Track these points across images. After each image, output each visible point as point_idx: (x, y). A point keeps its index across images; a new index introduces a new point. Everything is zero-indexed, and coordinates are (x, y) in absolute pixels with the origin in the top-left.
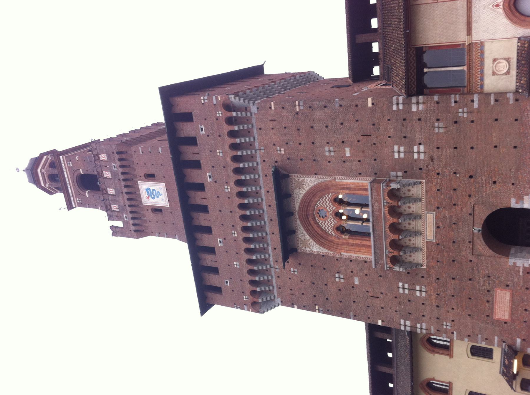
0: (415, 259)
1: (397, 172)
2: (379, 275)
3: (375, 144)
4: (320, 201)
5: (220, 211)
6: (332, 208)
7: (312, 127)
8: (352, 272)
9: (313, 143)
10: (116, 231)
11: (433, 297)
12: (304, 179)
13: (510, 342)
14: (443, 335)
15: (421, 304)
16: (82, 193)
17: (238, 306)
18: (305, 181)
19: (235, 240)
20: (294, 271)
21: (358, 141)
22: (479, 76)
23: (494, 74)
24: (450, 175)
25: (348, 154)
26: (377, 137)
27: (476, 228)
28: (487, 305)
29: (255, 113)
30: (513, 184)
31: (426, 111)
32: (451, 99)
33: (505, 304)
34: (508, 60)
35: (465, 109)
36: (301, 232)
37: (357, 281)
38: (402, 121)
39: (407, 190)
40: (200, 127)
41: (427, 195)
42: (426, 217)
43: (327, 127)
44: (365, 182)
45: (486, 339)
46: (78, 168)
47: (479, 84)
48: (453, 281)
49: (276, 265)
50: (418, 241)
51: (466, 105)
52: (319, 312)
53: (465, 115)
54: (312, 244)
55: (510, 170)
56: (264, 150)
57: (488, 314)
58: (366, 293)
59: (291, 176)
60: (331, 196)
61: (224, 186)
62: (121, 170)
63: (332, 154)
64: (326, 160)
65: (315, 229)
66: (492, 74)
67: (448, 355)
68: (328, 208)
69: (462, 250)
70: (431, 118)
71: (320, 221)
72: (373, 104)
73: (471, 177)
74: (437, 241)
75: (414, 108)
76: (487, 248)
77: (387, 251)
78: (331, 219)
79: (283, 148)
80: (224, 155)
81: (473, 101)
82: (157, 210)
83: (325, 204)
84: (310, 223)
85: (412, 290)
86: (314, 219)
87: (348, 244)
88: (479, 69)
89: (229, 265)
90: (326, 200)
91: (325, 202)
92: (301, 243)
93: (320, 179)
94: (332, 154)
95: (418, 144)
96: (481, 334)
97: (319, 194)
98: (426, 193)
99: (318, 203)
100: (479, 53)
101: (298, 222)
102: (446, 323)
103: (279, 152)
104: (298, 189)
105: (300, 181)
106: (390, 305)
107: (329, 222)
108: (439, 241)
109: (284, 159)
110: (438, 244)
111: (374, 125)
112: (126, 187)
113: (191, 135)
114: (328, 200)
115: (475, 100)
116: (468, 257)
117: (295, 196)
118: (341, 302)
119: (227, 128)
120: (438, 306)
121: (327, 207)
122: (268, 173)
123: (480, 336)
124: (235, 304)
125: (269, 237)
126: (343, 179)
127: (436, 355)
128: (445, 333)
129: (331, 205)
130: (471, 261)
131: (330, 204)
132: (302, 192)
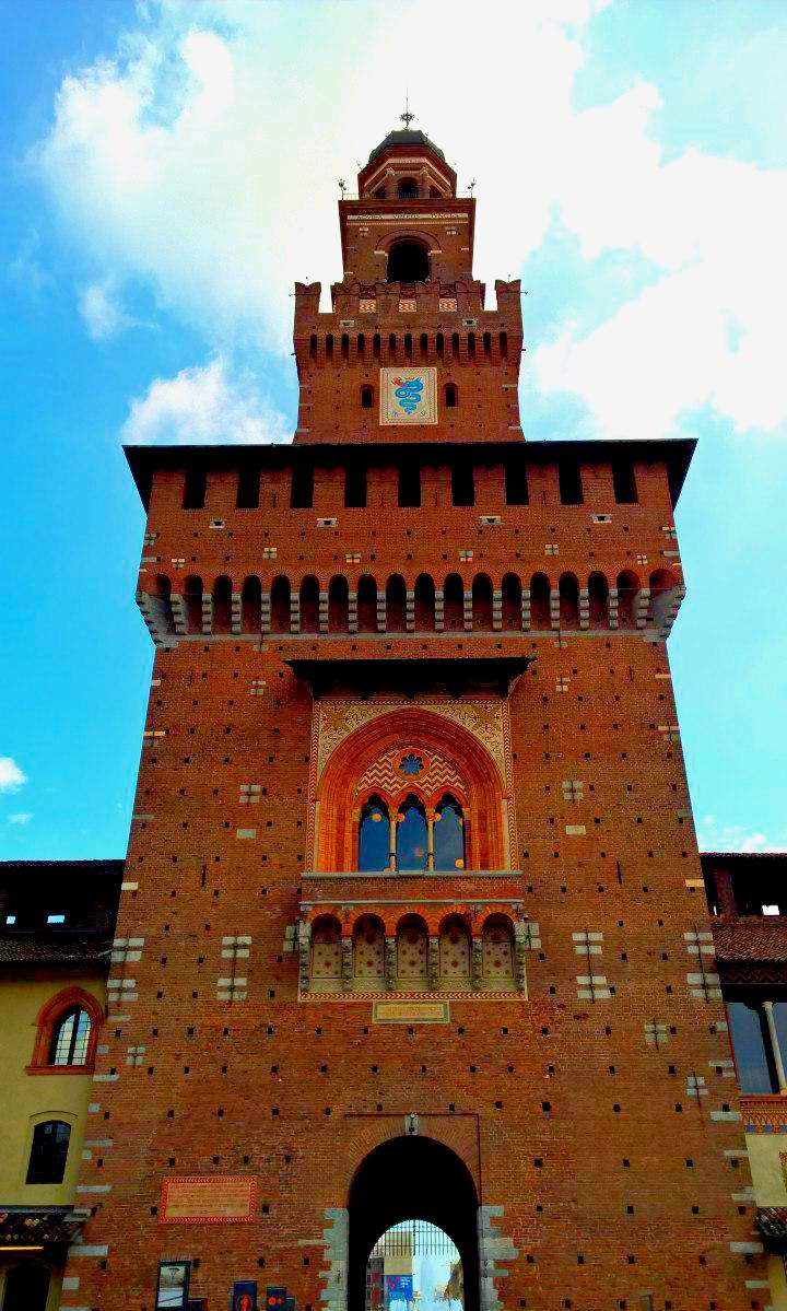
1: (539, 937)
3: (601, 890)
7: (624, 756)
8: (269, 824)
10: (306, 295)
11: (217, 1020)
12: (499, 729)
13: (95, 1226)
15: (195, 989)
16: (386, 241)
17: (152, 543)
18: (497, 732)
20: (257, 687)
21: (603, 855)
22: (775, 1122)
24: (545, 1057)
25: (570, 830)
26: (618, 896)
27: (416, 1121)
28: (207, 1159)
30: (539, 1209)
35: (704, 1092)
37: (244, 834)
40: (608, 516)
41: (492, 1004)
42: (435, 1003)
43: (629, 788)
44: (508, 866)
45: (100, 1163)
50: (366, 984)
51: (714, 1093)
52: (145, 738)
54: (336, 736)
55: (574, 1201)
57: (177, 1161)
62: (463, 334)
63: (567, 796)
67: (35, 1062)
69: (356, 1088)
72: (692, 889)
73: (546, 1107)
75: (694, 978)
76: (366, 1151)
80: (548, 557)
81: (726, 1108)
82: (369, 397)
83: (437, 774)
85: (234, 967)
87: (341, 819)
94: (567, 796)
97: (463, 762)
101: (391, 708)
106: (185, 912)
107: (391, 778)
110: (366, 1031)
112: (424, 337)
113: (585, 493)
114: (447, 780)
117: (456, 706)
119: (611, 572)
120: (191, 1031)
123: (110, 1143)
124: (158, 535)
125: (343, 636)
127: (35, 1030)
130: (328, 1112)
132: (467, 721)
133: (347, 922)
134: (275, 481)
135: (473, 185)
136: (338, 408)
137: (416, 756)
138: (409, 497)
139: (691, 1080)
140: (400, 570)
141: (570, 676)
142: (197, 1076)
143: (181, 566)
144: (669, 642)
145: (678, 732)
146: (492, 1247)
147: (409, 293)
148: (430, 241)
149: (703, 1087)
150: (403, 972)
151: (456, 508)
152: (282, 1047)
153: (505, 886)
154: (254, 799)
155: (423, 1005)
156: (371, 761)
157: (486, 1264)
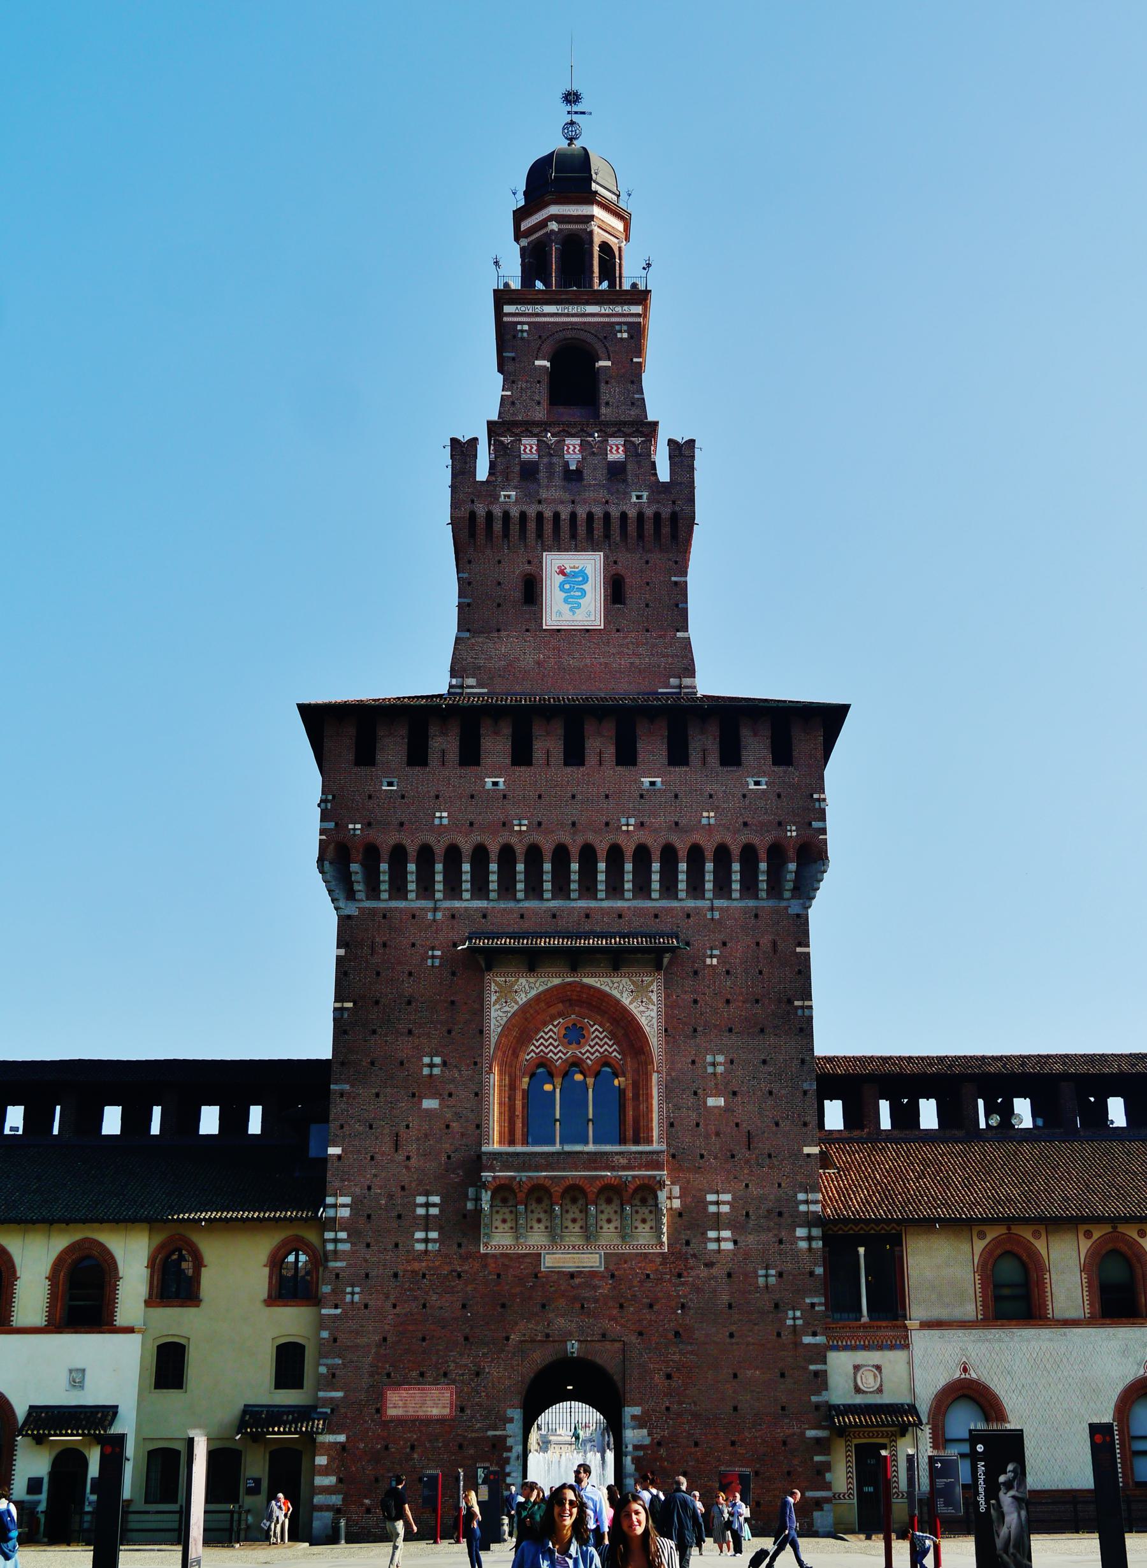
2: (453, 1155)
3: (733, 1156)
4: (603, 1031)
5: (573, 797)
6: (588, 1058)
7: (762, 1030)
8: (450, 1095)
9: (730, 1030)
10: (462, 452)
11: (416, 1266)
14: (329, 1287)
16: (547, 348)
17: (329, 805)
18: (651, 1007)
19: (504, 824)
20: (433, 957)
21: (737, 1125)
22: (853, 1342)
23: (857, 1368)
24: (679, 1296)
25: (711, 1102)
27: (576, 1345)
28: (414, 1374)
31: (796, 1253)
32: (817, 1297)
33: (421, 1407)
34: (880, 1390)
35: (799, 1322)
36: (533, 985)
37: (429, 1104)
38: (777, 1210)
39: (644, 1216)
40: (763, 780)
43: (764, 1062)
47: (840, 1343)
48: (459, 1305)
49: (444, 915)
50: (536, 1239)
51: (807, 1324)
52: (335, 1009)
53: (789, 1322)
56: (712, 919)
58: (405, 1124)
62: (632, 513)
66: (856, 1364)
72: (809, 1155)
74: (543, 1274)
75: (801, 1232)
77: (524, 1179)
78: (565, 1054)
79: (718, 962)
81: (814, 1334)
83: (597, 1043)
85: (427, 1223)
86: (561, 1015)
88: (864, 1342)
89: (437, 797)
90: (606, 1046)
92: (506, 982)
93: (656, 1040)
95: (735, 1238)
96: (343, 1364)
98: (641, 1253)
99: (596, 1026)
100: (891, 1342)
101: (557, 981)
102: (357, 1293)
103: (709, 952)
104: (632, 987)
108: (543, 1277)
109: (694, 962)
110: (536, 1276)
113: (744, 753)
114: (606, 1050)
115: (817, 1338)
116: (515, 1333)
117: (615, 980)
118: (372, 1063)
120: (396, 1275)
121: (590, 1046)
124: (334, 797)
125: (511, 904)
126: (659, 1089)
127: (267, 1270)
128: (333, 1290)
129: (595, 1056)
132: (625, 995)
133: (521, 1191)
134: (444, 734)
135: (649, 265)
136: (499, 605)
137: (579, 1026)
138: (574, 756)
139: (790, 1313)
140: (565, 838)
141: (720, 948)
142: (403, 1311)
143: (358, 832)
145: (811, 1007)
146: (633, 1436)
147: (573, 431)
148: (598, 346)
149: (798, 1318)
150: (567, 1227)
151: (619, 768)
152: (469, 1288)
154: (436, 1071)
156: (538, 1031)
157: (627, 1447)
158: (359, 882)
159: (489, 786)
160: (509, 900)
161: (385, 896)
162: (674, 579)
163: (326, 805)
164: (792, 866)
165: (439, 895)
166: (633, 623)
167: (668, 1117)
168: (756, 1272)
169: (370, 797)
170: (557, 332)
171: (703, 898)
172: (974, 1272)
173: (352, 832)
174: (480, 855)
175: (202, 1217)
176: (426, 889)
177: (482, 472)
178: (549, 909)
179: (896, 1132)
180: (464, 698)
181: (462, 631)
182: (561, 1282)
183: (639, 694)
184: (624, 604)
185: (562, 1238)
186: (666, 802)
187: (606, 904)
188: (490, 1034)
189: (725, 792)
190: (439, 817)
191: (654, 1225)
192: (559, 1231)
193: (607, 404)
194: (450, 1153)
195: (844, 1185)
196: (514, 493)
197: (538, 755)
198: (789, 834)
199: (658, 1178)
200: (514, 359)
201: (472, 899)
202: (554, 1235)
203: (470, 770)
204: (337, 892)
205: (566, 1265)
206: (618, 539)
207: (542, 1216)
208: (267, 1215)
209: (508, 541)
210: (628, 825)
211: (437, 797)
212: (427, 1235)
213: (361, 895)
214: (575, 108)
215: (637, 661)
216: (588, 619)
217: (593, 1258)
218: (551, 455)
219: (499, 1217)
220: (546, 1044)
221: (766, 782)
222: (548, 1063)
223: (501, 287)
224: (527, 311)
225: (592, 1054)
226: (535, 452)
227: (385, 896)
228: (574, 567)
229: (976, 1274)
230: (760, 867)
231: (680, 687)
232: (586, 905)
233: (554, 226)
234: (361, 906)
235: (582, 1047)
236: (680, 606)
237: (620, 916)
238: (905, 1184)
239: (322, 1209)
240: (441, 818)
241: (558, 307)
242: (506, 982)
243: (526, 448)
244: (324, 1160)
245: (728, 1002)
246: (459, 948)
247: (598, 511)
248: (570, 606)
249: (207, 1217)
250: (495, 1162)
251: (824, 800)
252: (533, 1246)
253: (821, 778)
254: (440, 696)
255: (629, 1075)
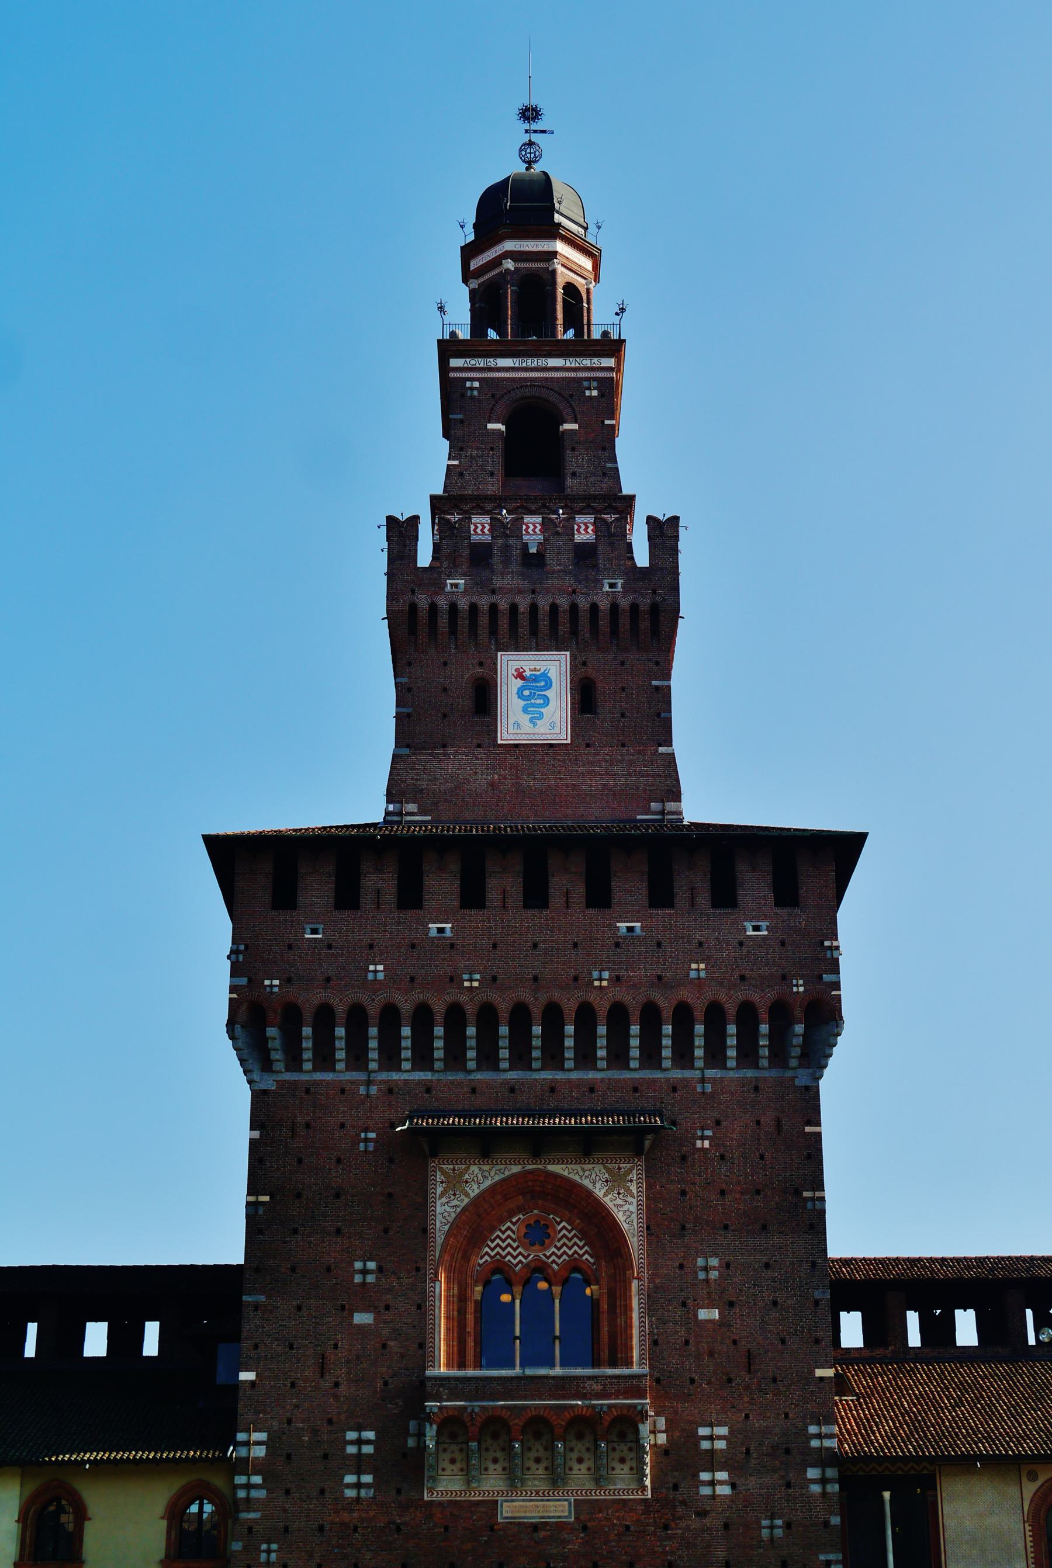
0: (445, 1473)
3: (730, 1381)
5: (535, 946)
7: (764, 1227)
8: (387, 1307)
11: (346, 1517)
17: (241, 958)
18: (630, 1199)
19: (452, 979)
24: (665, 1553)
25: (703, 1314)
29: (796, 1079)
36: (487, 1174)
37: (361, 1318)
40: (764, 924)
43: (767, 1266)
46: (579, 416)
49: (379, 1090)
52: (248, 1204)
54: (455, 1203)
56: (703, 1093)
58: (332, 1343)
59: (639, 1161)
60: (586, 1259)
61: (608, 969)
62: (604, 604)
64: (684, 1258)
65: (494, 1212)
68: (554, 1249)
70: (792, 1509)
71: (516, 1226)
72: (821, 1379)
75: (812, 1473)
77: (477, 1410)
78: (526, 1257)
79: (710, 1145)
83: (564, 1244)
84: (510, 1198)
86: (520, 1210)
89: (371, 946)
90: (576, 1248)
91: (570, 1244)
92: (454, 1170)
93: (636, 1239)
95: (733, 1481)
98: (619, 1499)
99: (564, 1224)
101: (516, 1169)
103: (699, 1133)
104: (607, 1175)
105: (629, 1184)
107: (515, 1249)
108: (500, 1530)
110: (492, 1529)
111: (774, 1380)
113: (740, 892)
114: (576, 1252)
117: (586, 1167)
120: (321, 1528)
121: (556, 1247)
122: (642, 1096)
124: (247, 947)
125: (460, 1076)
126: (639, 1299)
129: (562, 1259)
131: (565, 1257)
132: (598, 1185)
133: (473, 1425)
135: (623, 310)
136: (445, 716)
137: (542, 1223)
140: (525, 995)
141: (712, 1128)
143: (276, 990)
144: (822, 1083)
147: (533, 507)
148: (562, 405)
150: (528, 1469)
151: (590, 911)
153: (632, 1387)
154: (370, 1279)
155: (548, 1503)
158: (278, 1050)
159: (433, 933)
160: (458, 1071)
161: (308, 1066)
162: (654, 683)
163: (237, 958)
164: (799, 1028)
165: (373, 1066)
166: (607, 737)
167: (651, 1333)
168: (759, 1523)
169: (290, 947)
170: (514, 389)
171: (692, 1067)
172: (1024, 1522)
173: (268, 989)
174: (423, 1017)
175: (86, 1458)
176: (358, 1058)
177: (424, 557)
178: (506, 1082)
179: (926, 1350)
180: (403, 827)
181: (400, 747)
182: (522, 1536)
183: (613, 821)
184: (595, 713)
185: (523, 1482)
186: (646, 952)
187: (575, 1075)
188: (435, 1234)
189: (717, 939)
190: (372, 971)
191: (634, 1466)
192: (519, 1474)
193: (574, 474)
194: (387, 1378)
195: (865, 1415)
196: (463, 581)
197: (493, 895)
198: (795, 989)
199: (639, 1408)
200: (462, 421)
201: (413, 1069)
202: (514, 1479)
203: (409, 914)
204: (251, 1061)
205: (528, 1514)
206: (587, 635)
207: (499, 1454)
208: (165, 1455)
209: (456, 638)
210: (601, 979)
211: (371, 946)
212: (359, 1478)
213: (279, 1066)
214: (534, 126)
215: (611, 782)
216: (552, 731)
217: (560, 1506)
218: (507, 536)
219: (447, 1456)
220: (503, 1245)
221: (767, 926)
222: (506, 1268)
223: (447, 337)
224: (477, 365)
225: (559, 1257)
226: (487, 532)
227: (308, 1066)
228: (535, 670)
229: (1027, 1525)
230: (760, 1029)
231: (662, 812)
232: (551, 1077)
233: (509, 264)
234: (279, 1079)
235: (548, 1247)
236: (663, 715)
237: (592, 1090)
238: (938, 1414)
239: (231, 1448)
240: (375, 972)
241: (515, 360)
242: (454, 1170)
243: (476, 527)
244: (237, 1386)
245: (723, 1193)
246: (398, 1129)
247: (563, 602)
248: (530, 716)
249: (92, 1458)
250: (441, 1389)
251: (837, 948)
252: (488, 1491)
253: (834, 922)
254: (374, 825)
255: (604, 1282)
